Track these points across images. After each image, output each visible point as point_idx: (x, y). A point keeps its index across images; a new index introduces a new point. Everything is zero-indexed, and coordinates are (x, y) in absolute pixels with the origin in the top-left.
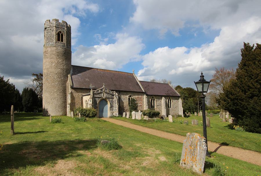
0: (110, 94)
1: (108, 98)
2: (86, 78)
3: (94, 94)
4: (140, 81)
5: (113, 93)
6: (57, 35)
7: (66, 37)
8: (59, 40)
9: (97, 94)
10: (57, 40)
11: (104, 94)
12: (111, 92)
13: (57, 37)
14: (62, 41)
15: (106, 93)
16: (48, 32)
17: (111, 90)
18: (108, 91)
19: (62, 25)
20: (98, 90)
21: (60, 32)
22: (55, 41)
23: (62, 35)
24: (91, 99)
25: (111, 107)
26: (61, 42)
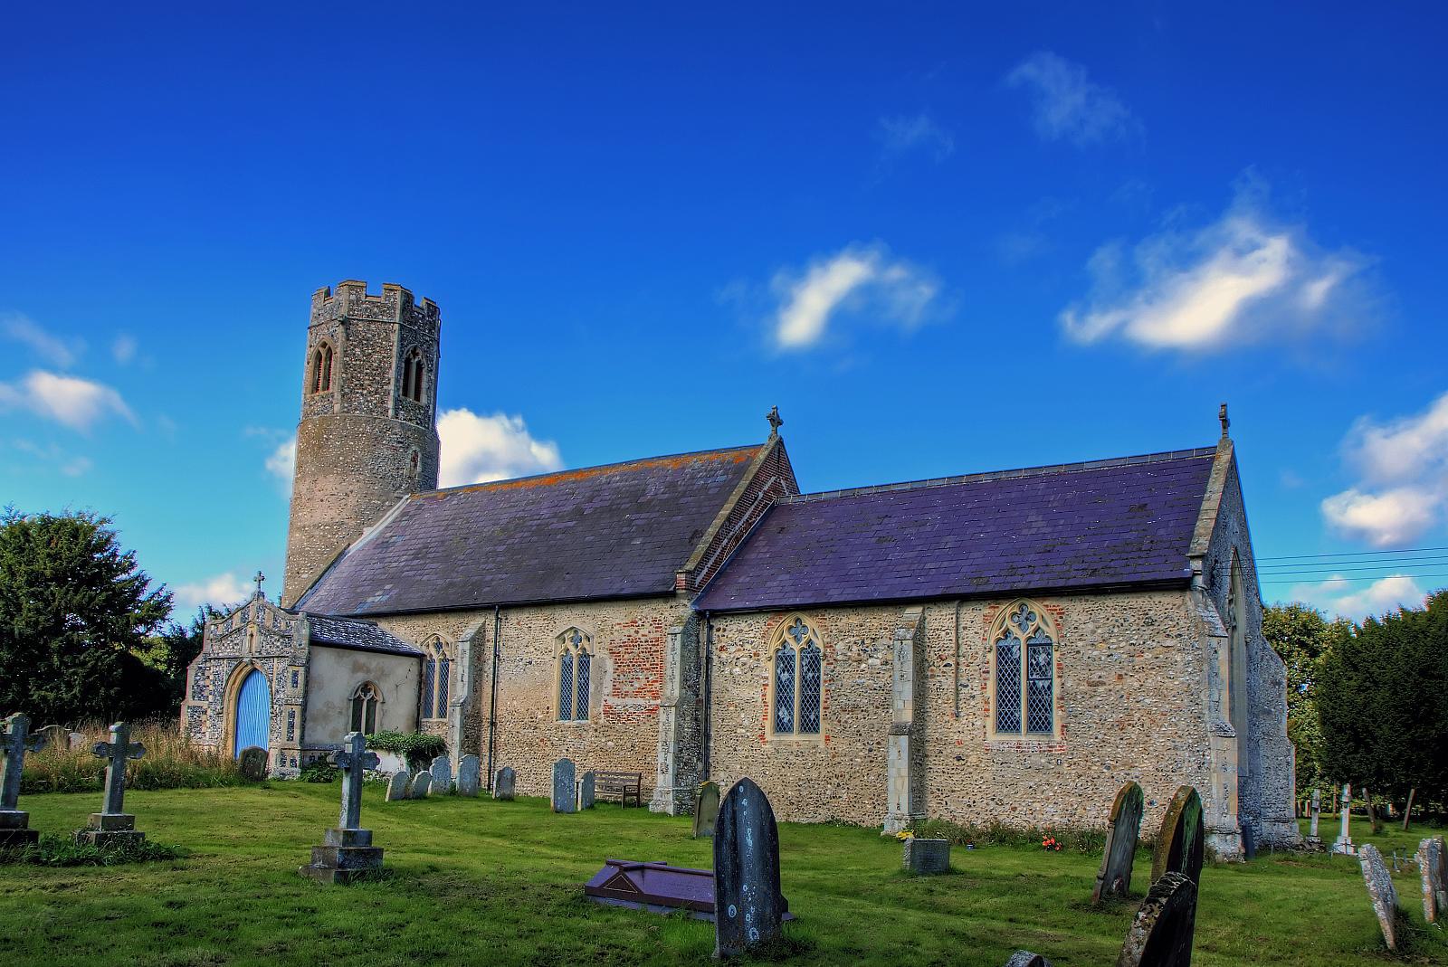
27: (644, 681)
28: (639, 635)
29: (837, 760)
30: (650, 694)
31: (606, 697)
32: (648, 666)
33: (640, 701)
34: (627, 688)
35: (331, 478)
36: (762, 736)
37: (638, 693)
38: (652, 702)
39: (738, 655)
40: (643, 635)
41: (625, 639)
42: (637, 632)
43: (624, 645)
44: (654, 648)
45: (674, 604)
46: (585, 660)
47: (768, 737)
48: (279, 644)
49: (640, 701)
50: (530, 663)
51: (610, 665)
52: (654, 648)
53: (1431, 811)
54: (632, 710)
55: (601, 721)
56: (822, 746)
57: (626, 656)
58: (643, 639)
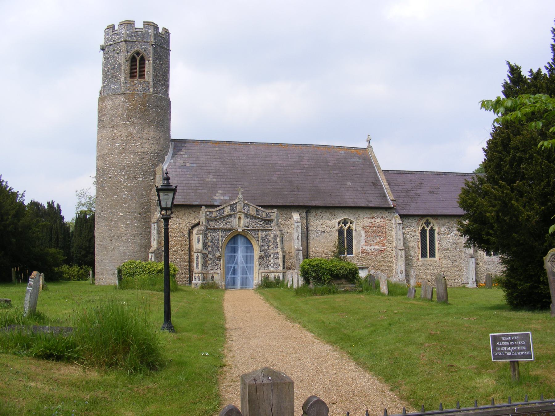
0: (259, 218)
1: (254, 230)
2: (209, 173)
3: (208, 220)
4: (386, 172)
5: (267, 214)
6: (128, 64)
7: (154, 62)
8: (132, 75)
9: (220, 219)
10: (128, 75)
11: (240, 218)
12: (263, 213)
13: (128, 68)
14: (142, 76)
15: (246, 215)
16: (108, 59)
17: (262, 206)
18: (253, 212)
19: (143, 35)
20: (223, 208)
21: (138, 53)
22: (123, 80)
23: (143, 60)
24: (201, 236)
25: (261, 258)
26: (140, 80)
27: (379, 240)
28: (376, 223)
29: (443, 266)
30: (381, 245)
31: (363, 246)
32: (380, 234)
33: (377, 247)
34: (372, 242)
35: (152, 128)
36: (418, 259)
37: (376, 244)
38: (382, 248)
39: (409, 230)
40: (377, 223)
41: (370, 224)
42: (375, 221)
43: (369, 226)
44: (382, 228)
45: (390, 211)
46: (350, 231)
47: (420, 259)
48: (261, 223)
49: (377, 247)
50: (324, 232)
51: (363, 233)
52: (382, 228)
53: (128, 223)
54: (374, 251)
55: (360, 255)
56: (438, 262)
57: (370, 230)
58: (378, 224)
